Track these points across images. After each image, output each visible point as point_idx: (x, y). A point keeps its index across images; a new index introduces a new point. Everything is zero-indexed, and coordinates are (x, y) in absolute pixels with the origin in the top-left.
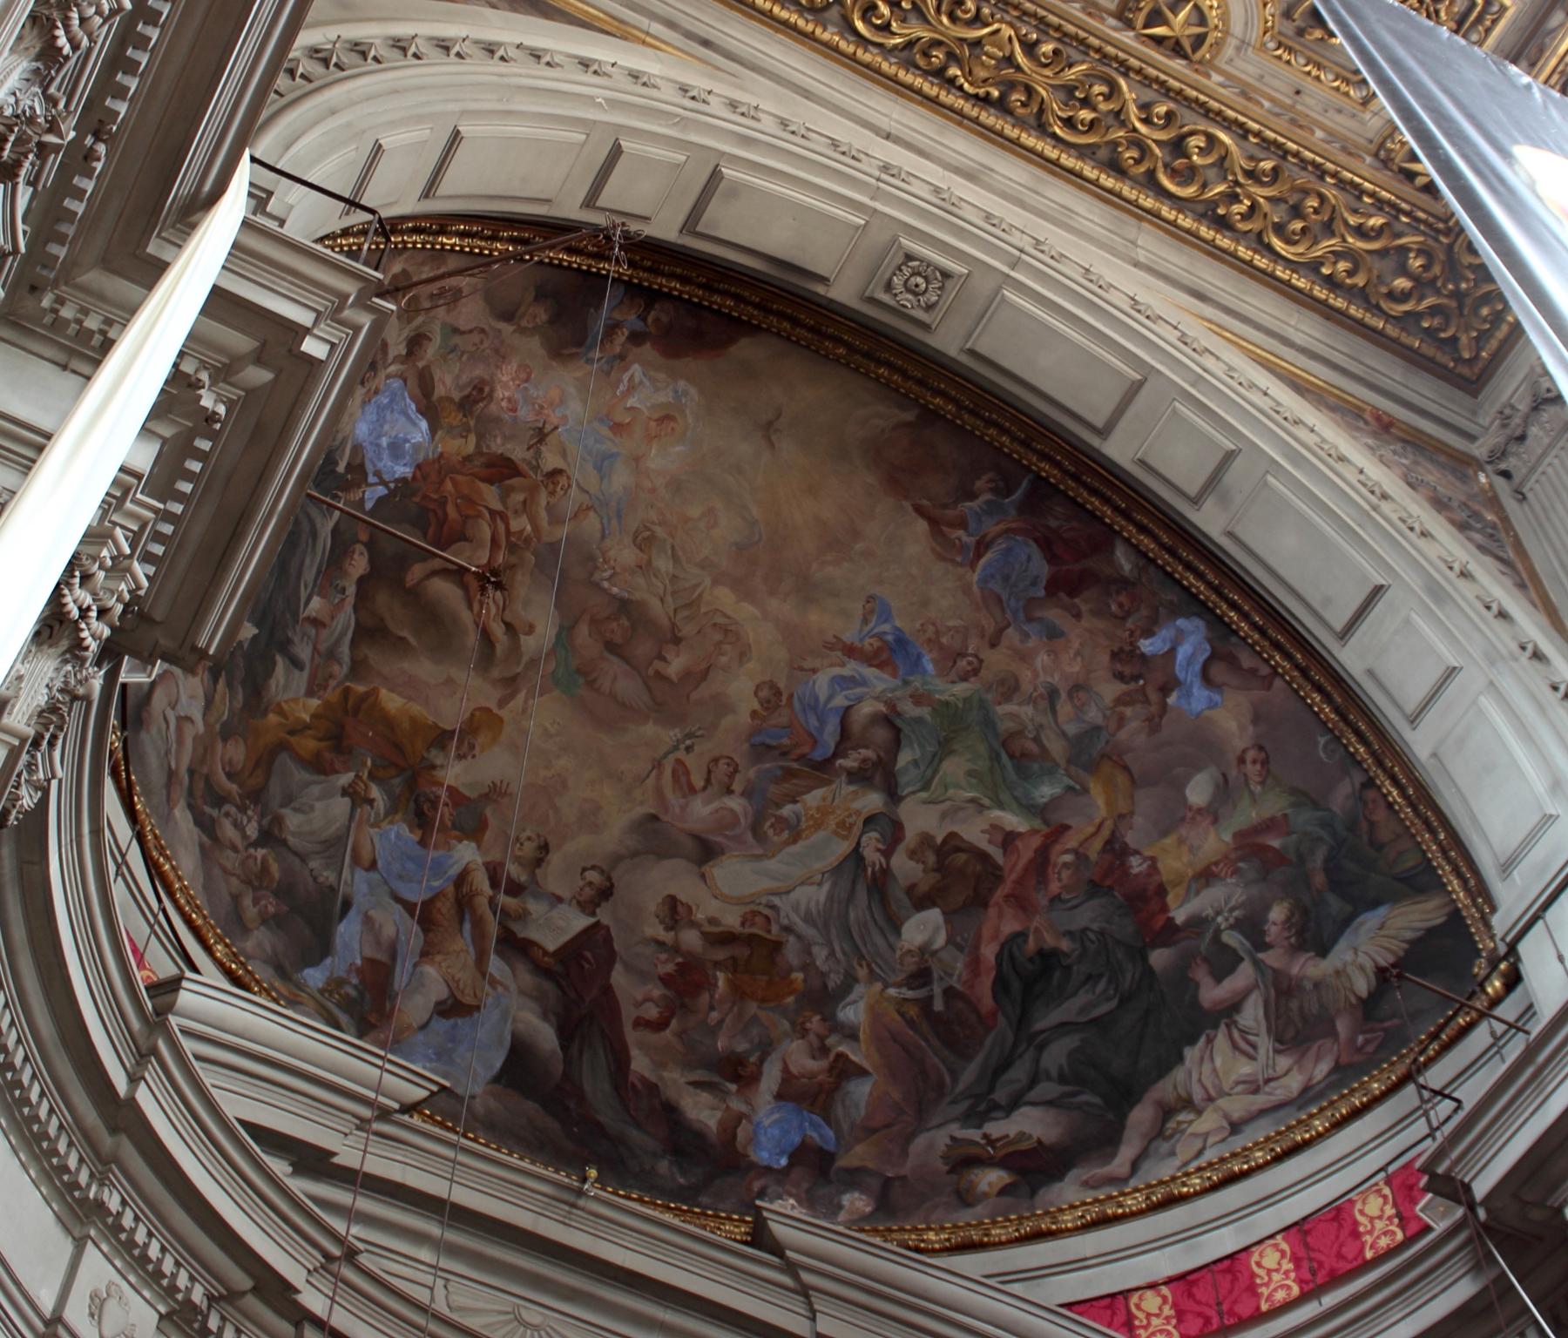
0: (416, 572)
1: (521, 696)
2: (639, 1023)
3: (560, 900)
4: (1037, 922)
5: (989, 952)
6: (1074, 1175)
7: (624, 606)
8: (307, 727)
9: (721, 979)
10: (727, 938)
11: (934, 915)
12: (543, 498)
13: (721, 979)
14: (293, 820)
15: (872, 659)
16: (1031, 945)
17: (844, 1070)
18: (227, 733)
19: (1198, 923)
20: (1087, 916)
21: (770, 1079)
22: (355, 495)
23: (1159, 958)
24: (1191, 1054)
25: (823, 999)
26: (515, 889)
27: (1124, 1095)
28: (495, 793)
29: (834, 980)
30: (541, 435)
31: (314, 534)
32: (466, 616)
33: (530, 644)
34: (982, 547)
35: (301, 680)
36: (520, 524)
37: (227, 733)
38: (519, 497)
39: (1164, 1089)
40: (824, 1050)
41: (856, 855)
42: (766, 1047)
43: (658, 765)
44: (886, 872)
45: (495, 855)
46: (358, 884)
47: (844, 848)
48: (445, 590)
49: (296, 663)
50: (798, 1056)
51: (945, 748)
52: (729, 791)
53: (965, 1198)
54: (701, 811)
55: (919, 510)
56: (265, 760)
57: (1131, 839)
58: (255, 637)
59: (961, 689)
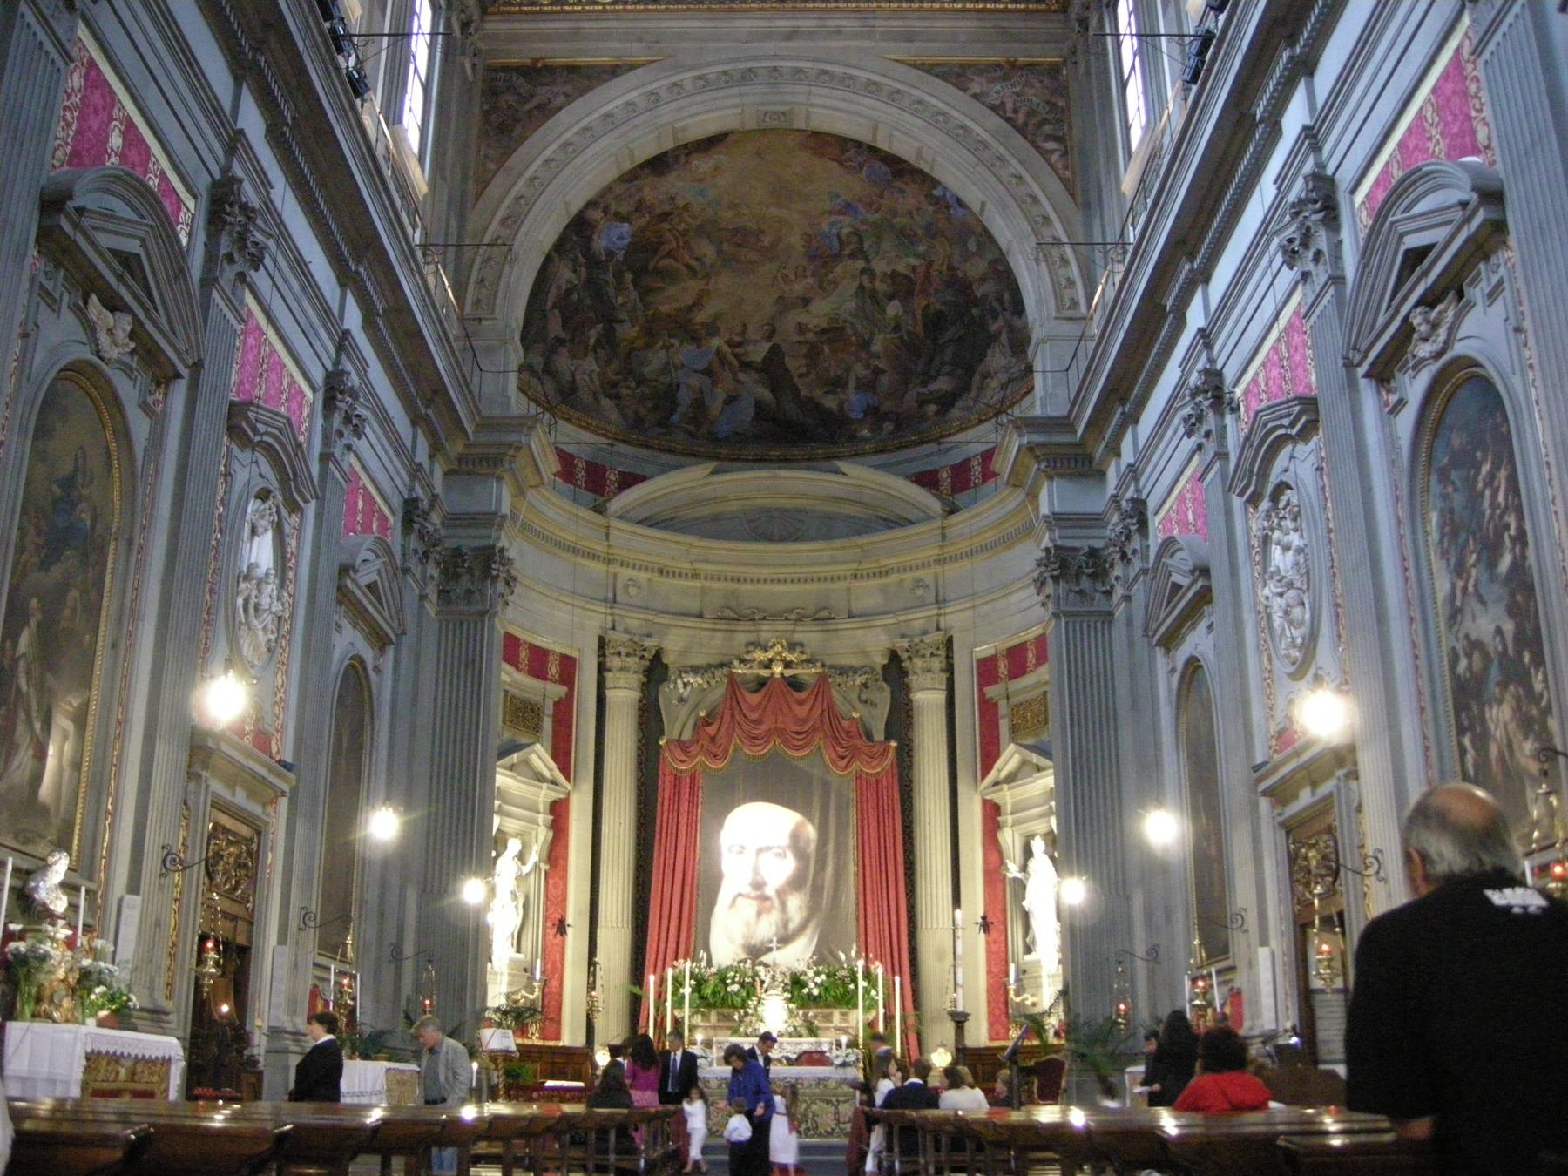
0: (651, 265)
1: (713, 281)
2: (801, 376)
4: (932, 300)
5: (919, 313)
6: (960, 404)
8: (637, 338)
9: (826, 349)
10: (824, 331)
11: (896, 302)
12: (685, 215)
13: (826, 349)
14: (647, 370)
15: (840, 213)
17: (877, 372)
18: (608, 362)
19: (985, 297)
20: (949, 297)
21: (852, 384)
23: (975, 311)
24: (989, 353)
25: (865, 345)
26: (740, 345)
27: (970, 370)
28: (718, 316)
29: (867, 337)
30: (672, 199)
33: (708, 261)
34: (861, 166)
36: (682, 227)
38: (676, 220)
39: (981, 368)
40: (868, 365)
41: (861, 287)
42: (848, 370)
43: (775, 278)
44: (874, 291)
45: (727, 337)
47: (856, 284)
48: (668, 262)
50: (860, 370)
51: (880, 238)
54: (798, 288)
55: (833, 160)
57: (955, 264)
58: (603, 328)
59: (877, 216)
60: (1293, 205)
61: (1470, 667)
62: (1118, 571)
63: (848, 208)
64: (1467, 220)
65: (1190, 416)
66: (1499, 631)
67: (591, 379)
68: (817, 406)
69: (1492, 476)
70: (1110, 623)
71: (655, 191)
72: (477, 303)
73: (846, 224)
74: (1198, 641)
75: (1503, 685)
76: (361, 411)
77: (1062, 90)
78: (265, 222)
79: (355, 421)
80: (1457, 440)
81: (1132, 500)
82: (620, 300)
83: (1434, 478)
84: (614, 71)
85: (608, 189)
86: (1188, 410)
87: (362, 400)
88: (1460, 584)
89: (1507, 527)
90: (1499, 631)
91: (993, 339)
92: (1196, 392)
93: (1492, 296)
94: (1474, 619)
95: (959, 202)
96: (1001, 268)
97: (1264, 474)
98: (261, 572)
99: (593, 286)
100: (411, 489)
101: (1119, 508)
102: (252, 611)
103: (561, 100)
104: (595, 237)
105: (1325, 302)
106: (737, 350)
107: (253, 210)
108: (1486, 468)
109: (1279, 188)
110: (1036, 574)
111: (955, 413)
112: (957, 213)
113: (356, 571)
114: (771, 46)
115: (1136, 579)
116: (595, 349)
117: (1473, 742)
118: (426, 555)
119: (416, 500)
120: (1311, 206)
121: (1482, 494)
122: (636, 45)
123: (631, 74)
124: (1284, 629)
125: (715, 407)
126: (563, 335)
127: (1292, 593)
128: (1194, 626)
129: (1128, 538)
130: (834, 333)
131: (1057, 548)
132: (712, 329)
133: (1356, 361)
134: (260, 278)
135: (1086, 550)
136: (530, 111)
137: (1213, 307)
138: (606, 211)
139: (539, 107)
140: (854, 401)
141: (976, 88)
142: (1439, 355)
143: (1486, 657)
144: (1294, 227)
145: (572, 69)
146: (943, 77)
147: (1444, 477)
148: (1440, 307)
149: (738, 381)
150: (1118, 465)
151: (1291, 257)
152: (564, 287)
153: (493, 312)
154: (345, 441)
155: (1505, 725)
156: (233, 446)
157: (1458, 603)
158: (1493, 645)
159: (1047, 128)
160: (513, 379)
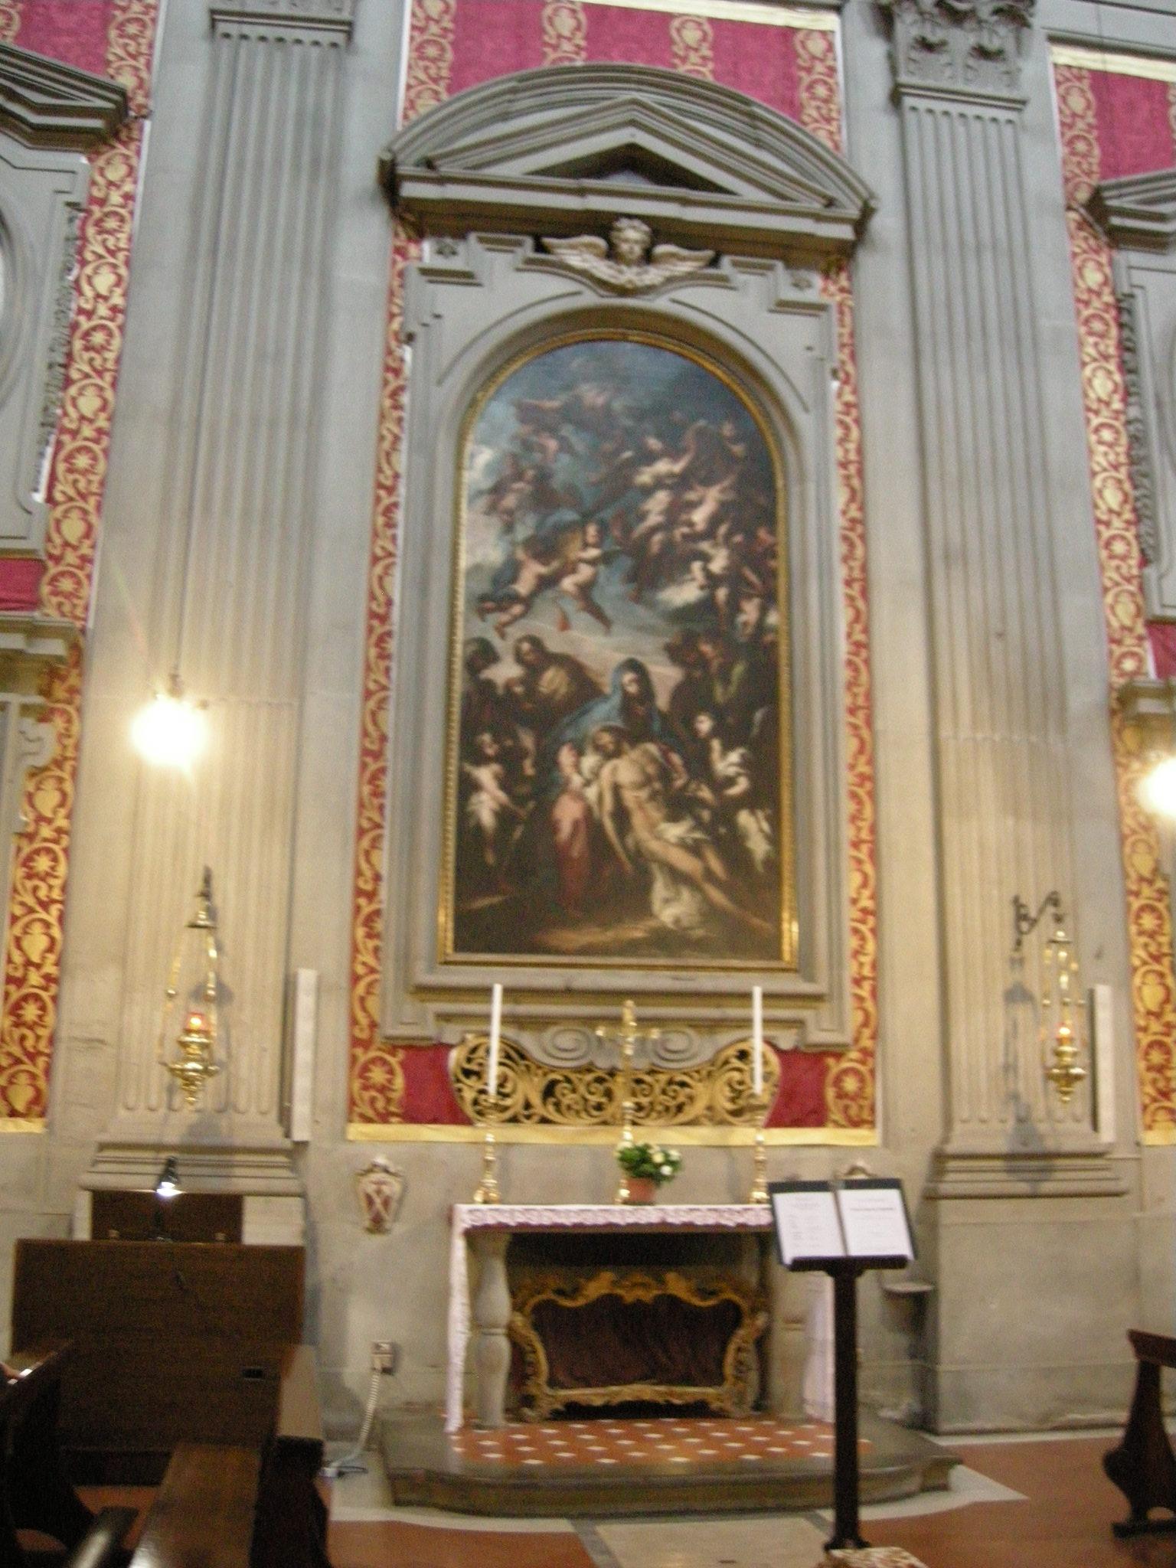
69: (680, 483)
121: (648, 491)
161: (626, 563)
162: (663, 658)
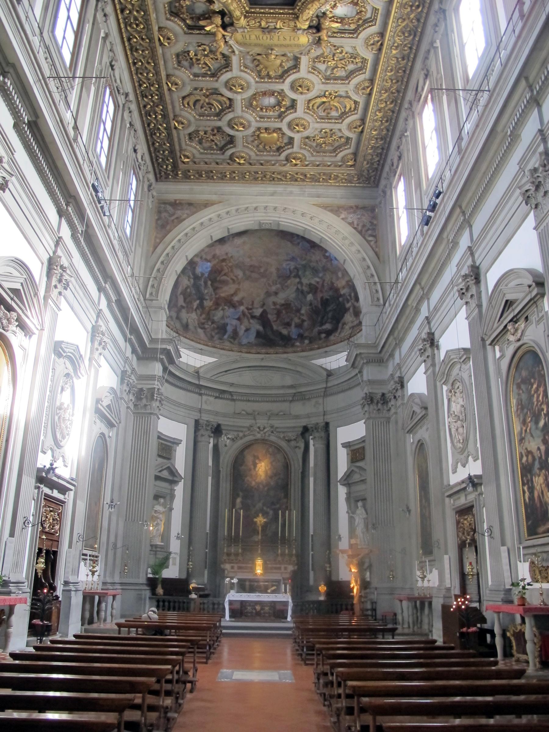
0: (218, 279)
3: (257, 308)
5: (319, 299)
7: (251, 266)
9: (284, 312)
10: (283, 305)
12: (232, 260)
13: (284, 312)
14: (216, 318)
16: (324, 298)
17: (303, 321)
18: (201, 315)
19: (344, 294)
20: (331, 293)
21: (293, 325)
22: (204, 277)
24: (346, 315)
25: (298, 310)
26: (251, 309)
28: (243, 298)
29: (299, 307)
30: (227, 254)
31: (201, 284)
32: (229, 279)
33: (240, 277)
34: (298, 244)
35: (208, 301)
36: (230, 264)
37: (201, 315)
39: (342, 321)
41: (298, 289)
42: (292, 320)
46: (227, 321)
47: (295, 288)
48: (225, 278)
49: (206, 300)
50: (297, 320)
51: (305, 271)
52: (276, 284)
53: (320, 339)
54: (274, 288)
56: (208, 314)
60: (463, 276)
61: (527, 460)
62: (393, 402)
63: (293, 259)
64: (530, 292)
65: (421, 349)
66: (539, 449)
67: (194, 321)
68: (280, 333)
69: (537, 389)
70: (389, 422)
71: (220, 251)
72: (151, 294)
73: (292, 265)
74: (423, 433)
75: (541, 469)
76: (105, 339)
77: (374, 217)
78: (70, 271)
79: (103, 344)
80: (524, 373)
81: (399, 377)
82: (206, 291)
83: (515, 387)
84: (206, 205)
85: (203, 250)
86: (421, 347)
87: (106, 335)
88: (524, 428)
89: (543, 410)
90: (539, 449)
91: (346, 310)
92: (424, 340)
93: (538, 322)
94: (529, 443)
95: (336, 259)
96: (350, 283)
97: (448, 375)
98: (65, 406)
99: (196, 286)
100: (125, 367)
101: (393, 378)
102: (62, 421)
103: (185, 216)
104: (197, 268)
105: (474, 314)
106: (250, 311)
107: (65, 268)
108: (535, 386)
109: (458, 269)
110: (362, 402)
111: (332, 338)
112: (334, 262)
113: (102, 401)
114: (266, 198)
115: (399, 407)
116: (196, 310)
117: (529, 488)
118: (129, 392)
119: (126, 371)
120: (470, 278)
121: (533, 396)
122: (214, 196)
123: (212, 207)
124: (456, 436)
125: (241, 332)
126: (184, 305)
127: (459, 422)
128: (421, 427)
129: (397, 390)
130: (287, 306)
131: (370, 393)
132: (241, 303)
133: (486, 339)
134: (68, 293)
135: (381, 394)
136: (173, 221)
137: (431, 309)
138: (201, 258)
139: (177, 218)
140: (294, 332)
141: (343, 216)
142: (519, 340)
143: (534, 457)
144: (463, 284)
145: (190, 204)
146: (331, 211)
147: (519, 387)
148: (519, 323)
149: (250, 323)
150: (393, 364)
151: (462, 295)
152: (185, 286)
153: (157, 297)
154: (99, 352)
155: (541, 485)
156: (56, 358)
157: (523, 435)
158: (537, 454)
159: (370, 232)
160: (165, 323)
161: (534, 418)
162: (542, 444)
